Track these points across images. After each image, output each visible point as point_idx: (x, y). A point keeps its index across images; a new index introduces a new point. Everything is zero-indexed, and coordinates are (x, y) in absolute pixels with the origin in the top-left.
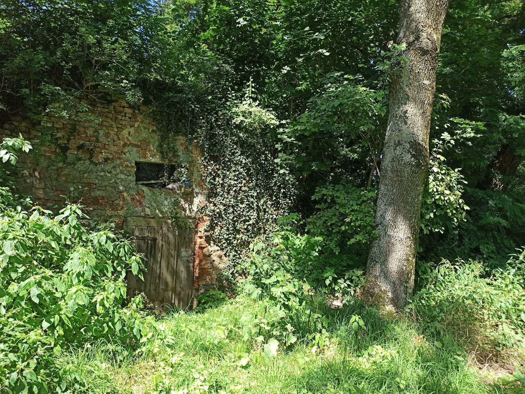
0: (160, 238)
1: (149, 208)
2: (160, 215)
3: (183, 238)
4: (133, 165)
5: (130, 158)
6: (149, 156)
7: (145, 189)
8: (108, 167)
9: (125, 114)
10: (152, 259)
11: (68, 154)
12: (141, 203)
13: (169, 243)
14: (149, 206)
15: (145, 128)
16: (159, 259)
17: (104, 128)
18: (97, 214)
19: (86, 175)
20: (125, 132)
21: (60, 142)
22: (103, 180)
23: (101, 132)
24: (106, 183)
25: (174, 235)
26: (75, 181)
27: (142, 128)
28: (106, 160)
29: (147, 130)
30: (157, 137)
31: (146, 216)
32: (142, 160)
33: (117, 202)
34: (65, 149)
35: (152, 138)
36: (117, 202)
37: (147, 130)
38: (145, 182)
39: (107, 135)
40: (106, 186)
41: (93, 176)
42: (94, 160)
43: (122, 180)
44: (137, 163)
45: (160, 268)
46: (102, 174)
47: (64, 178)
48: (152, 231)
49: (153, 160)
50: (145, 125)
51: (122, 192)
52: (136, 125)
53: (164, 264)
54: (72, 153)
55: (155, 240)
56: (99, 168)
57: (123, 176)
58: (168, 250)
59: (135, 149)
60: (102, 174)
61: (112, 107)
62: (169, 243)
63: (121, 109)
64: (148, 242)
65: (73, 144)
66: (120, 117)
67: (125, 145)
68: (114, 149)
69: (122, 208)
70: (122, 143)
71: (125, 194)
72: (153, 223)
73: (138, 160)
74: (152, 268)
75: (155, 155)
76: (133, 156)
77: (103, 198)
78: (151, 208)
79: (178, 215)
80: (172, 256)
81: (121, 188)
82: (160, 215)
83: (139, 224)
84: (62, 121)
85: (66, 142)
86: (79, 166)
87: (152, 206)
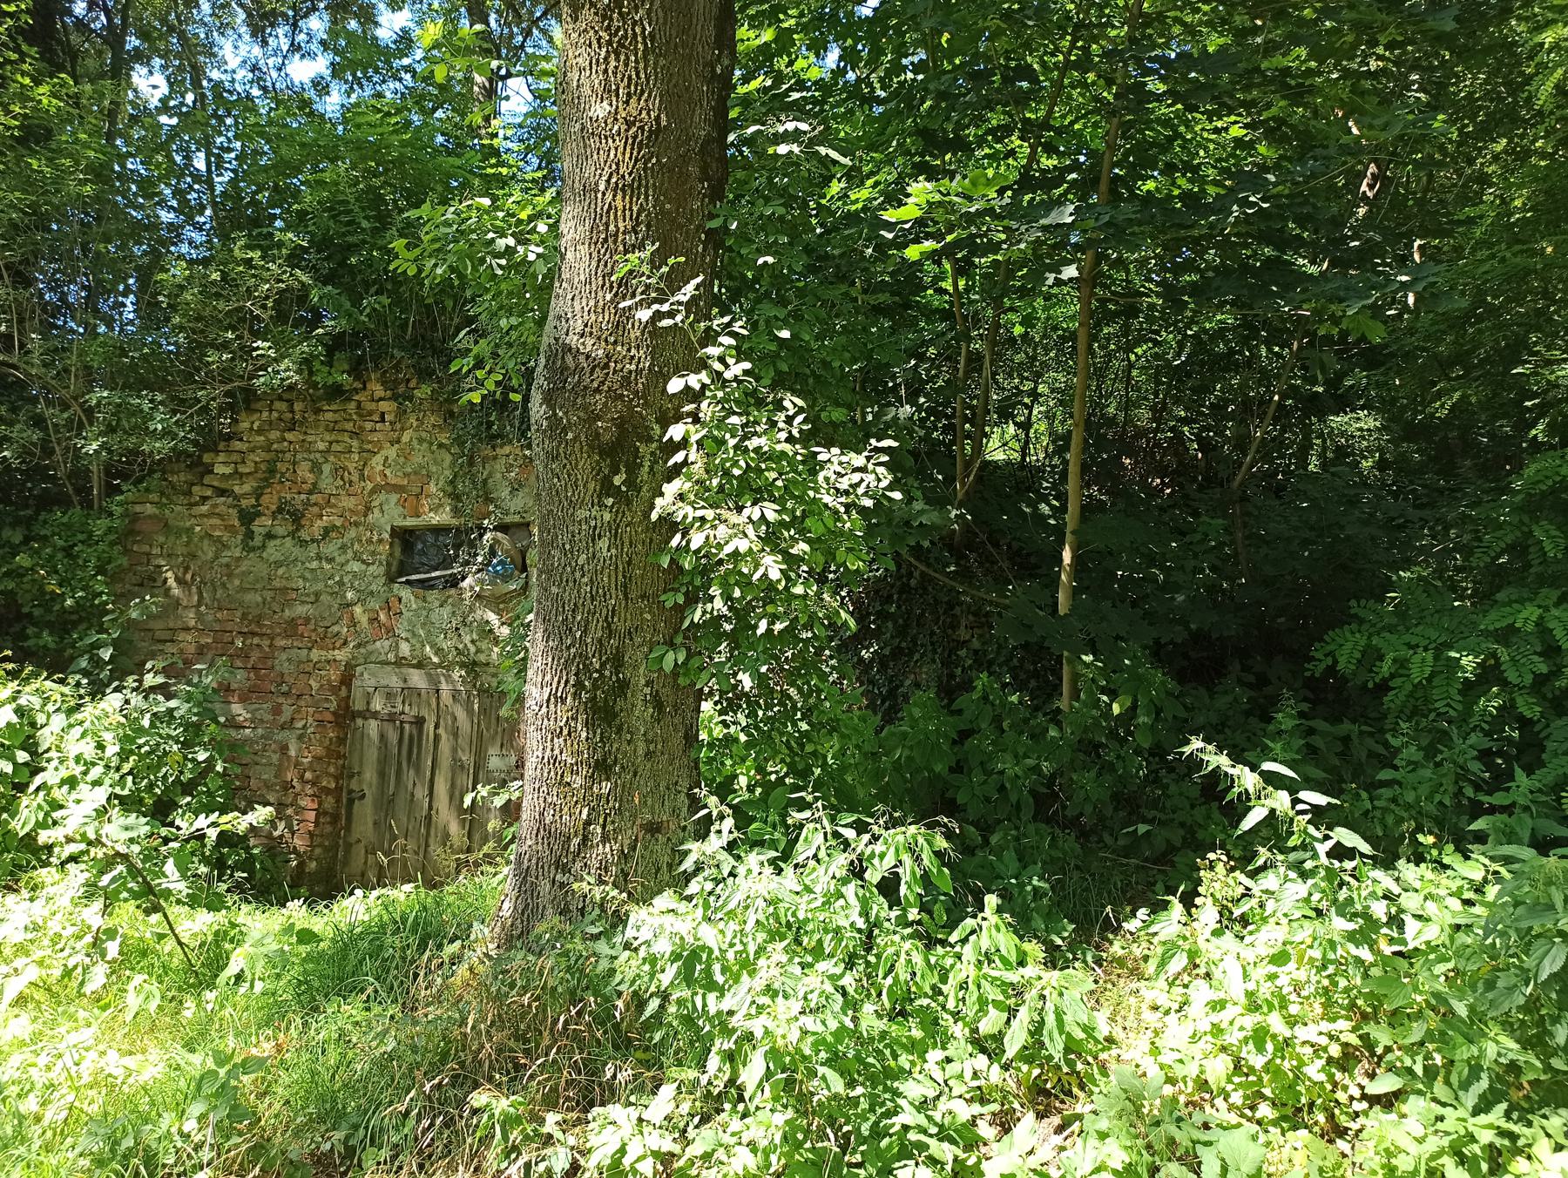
0: (434, 718)
1: (407, 640)
2: (435, 660)
3: (493, 721)
4: (386, 536)
5: (383, 520)
6: (426, 509)
7: (406, 593)
8: (330, 549)
9: (383, 415)
10: (412, 772)
11: (254, 528)
12: (390, 630)
13: (455, 734)
14: (409, 635)
15: (421, 441)
16: (428, 774)
17: (332, 458)
18: (289, 660)
19: (280, 571)
20: (377, 462)
21: (244, 503)
22: (316, 579)
23: (326, 468)
24: (320, 586)
25: (470, 711)
26: (258, 586)
27: (415, 442)
28: (327, 532)
29: (425, 445)
30: (448, 459)
31: (400, 662)
32: (410, 522)
33: (336, 629)
34: (247, 517)
35: (436, 462)
36: (336, 629)
37: (425, 445)
38: (414, 577)
39: (338, 471)
40: (317, 595)
41: (294, 572)
42: (304, 535)
43: (355, 575)
44: (395, 532)
45: (431, 794)
46: (315, 564)
47: (237, 582)
48: (415, 699)
49: (435, 519)
50: (424, 435)
51: (348, 605)
52: (405, 438)
53: (441, 787)
54: (262, 524)
55: (419, 722)
56: (313, 550)
57: (356, 566)
58: (454, 750)
59: (394, 497)
60: (315, 564)
61: (353, 405)
62: (455, 734)
63: (373, 406)
64: (402, 729)
65: (270, 501)
66: (368, 426)
67: (373, 491)
68: (348, 503)
69: (345, 643)
70: (370, 486)
71: (358, 610)
72: (417, 679)
73: (400, 522)
74: (412, 795)
75: (441, 505)
76: (390, 514)
77: (307, 620)
78: (413, 641)
79: (482, 658)
80: (462, 767)
81: (349, 595)
82: (435, 660)
83: (383, 682)
84: (252, 456)
85: (253, 501)
86: (273, 551)
87: (414, 635)
